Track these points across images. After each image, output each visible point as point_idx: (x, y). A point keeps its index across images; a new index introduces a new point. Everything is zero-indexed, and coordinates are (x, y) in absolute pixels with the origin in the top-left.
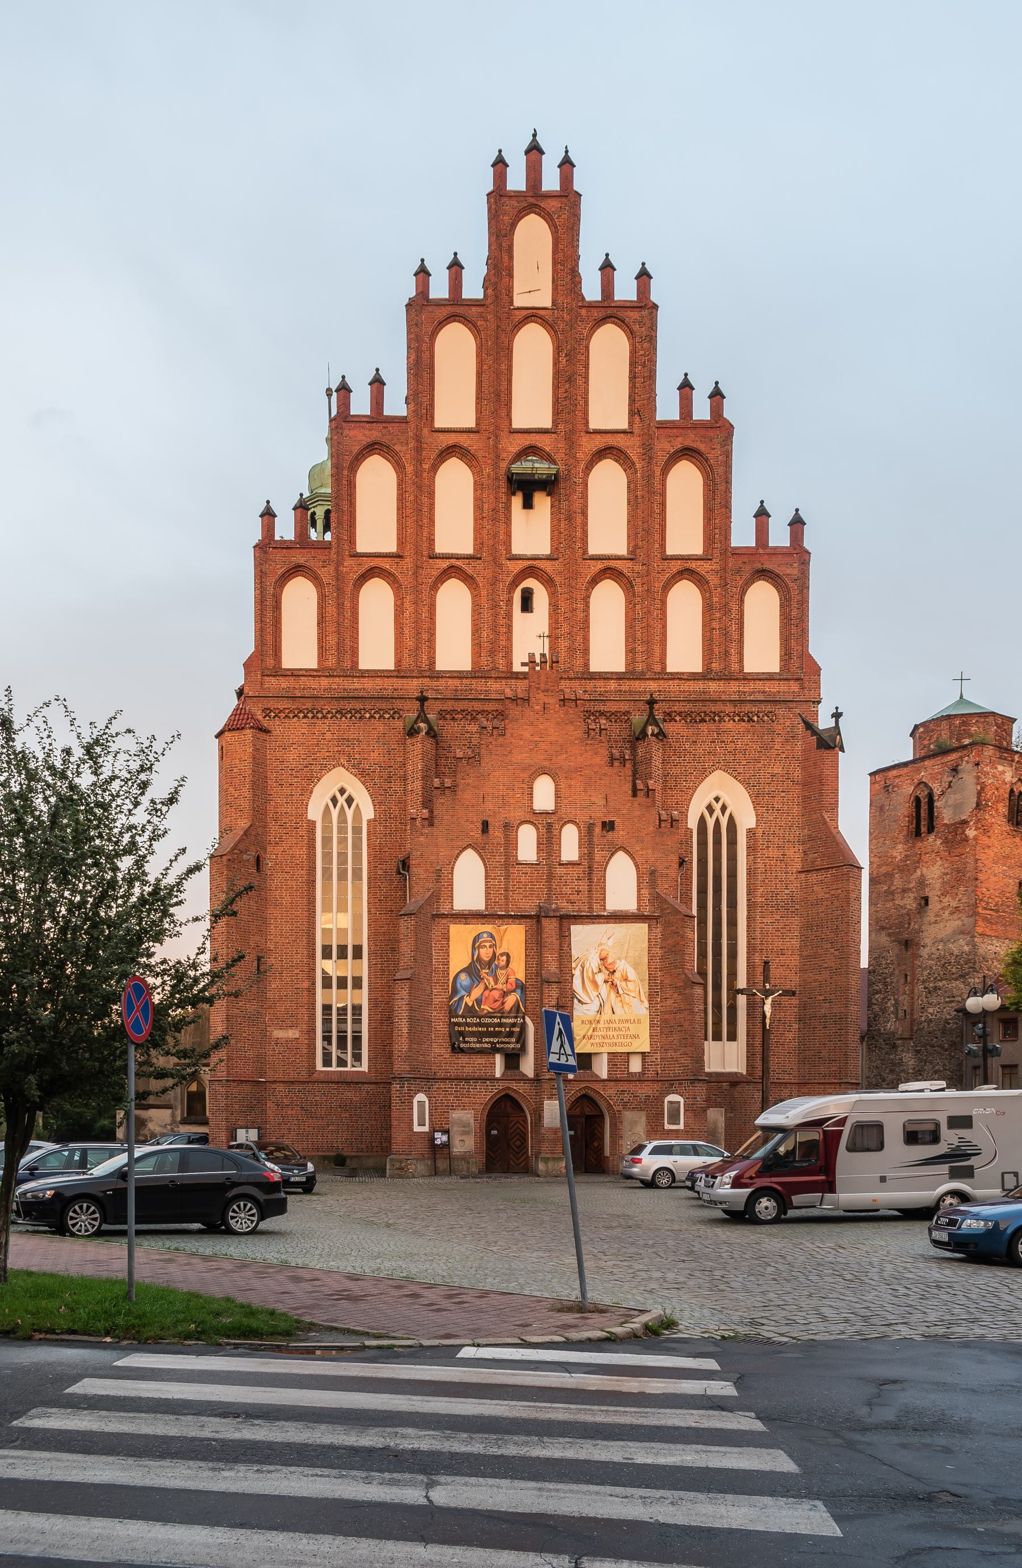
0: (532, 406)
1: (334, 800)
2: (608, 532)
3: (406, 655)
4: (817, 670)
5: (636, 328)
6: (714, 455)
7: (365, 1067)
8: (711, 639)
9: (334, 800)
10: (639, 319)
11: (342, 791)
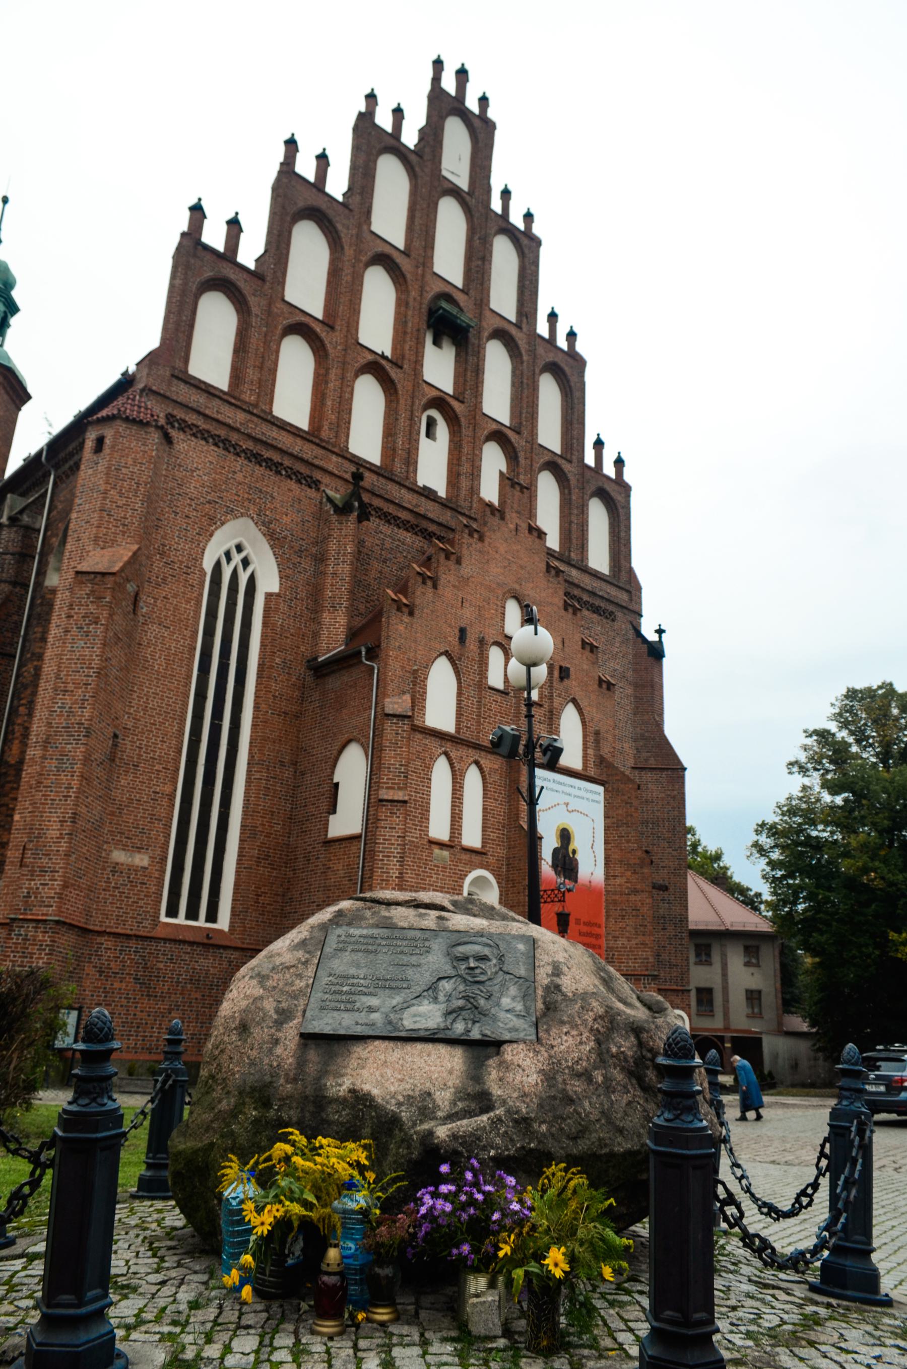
1: (228, 555)
3: (326, 427)
4: (639, 589)
5: (526, 251)
6: (573, 379)
7: (223, 922)
8: (570, 532)
9: (228, 555)
10: (527, 245)
11: (239, 548)
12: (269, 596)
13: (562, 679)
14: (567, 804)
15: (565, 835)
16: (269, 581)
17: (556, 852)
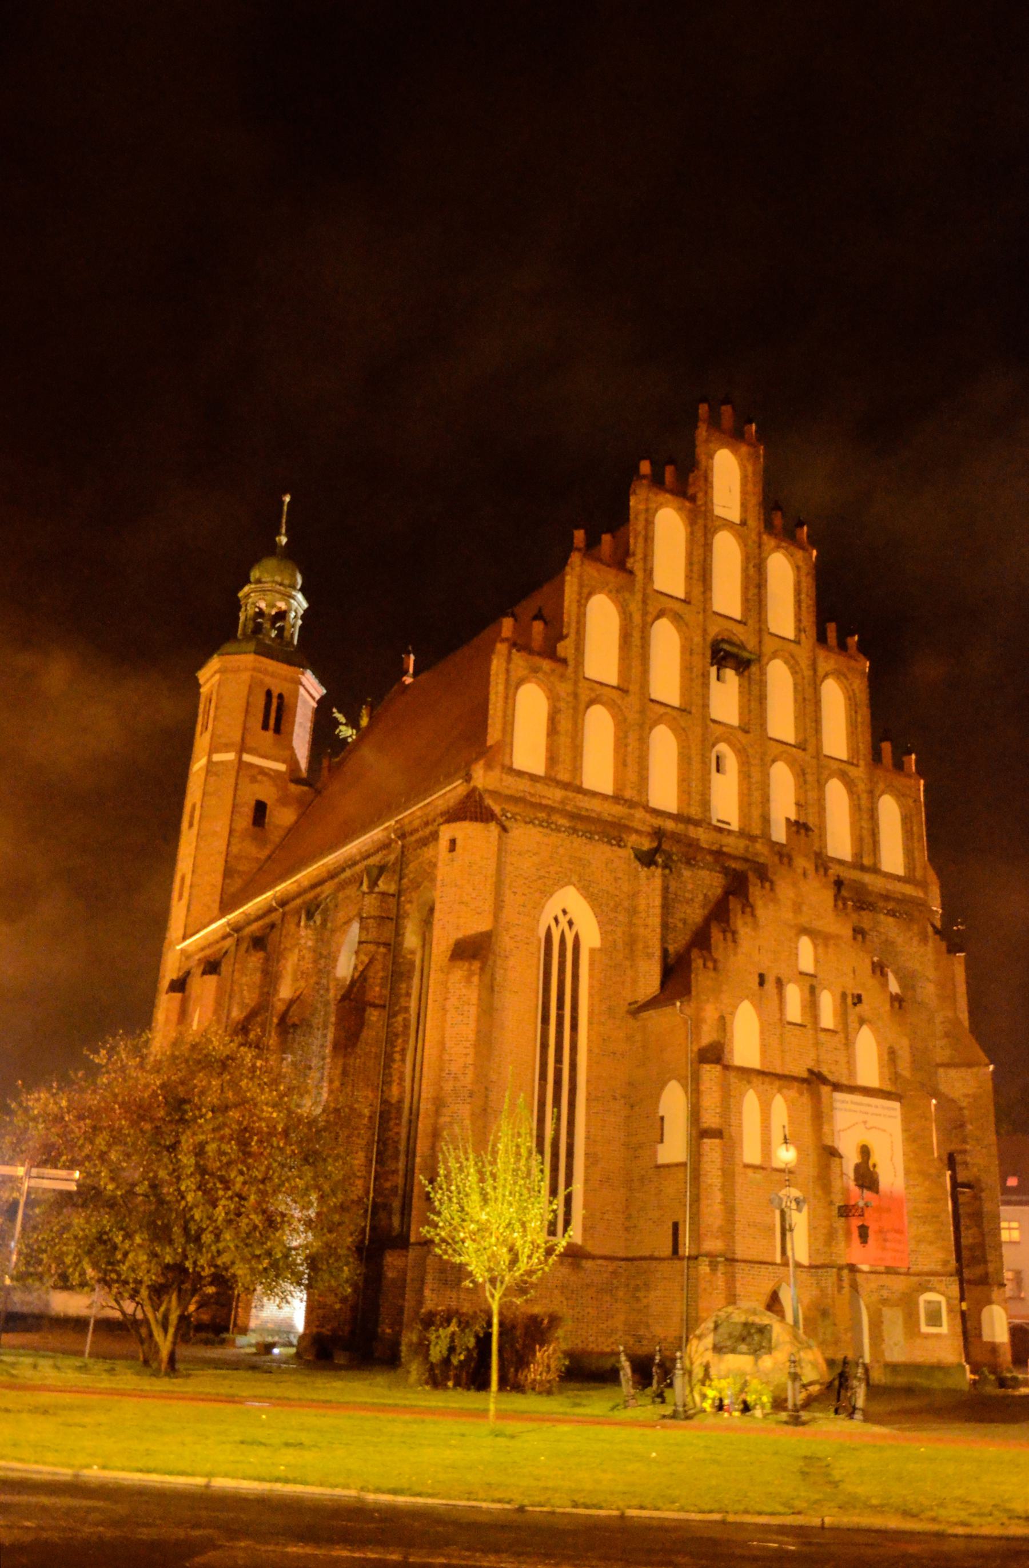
0: (727, 598)
1: (556, 919)
2: (782, 722)
11: (564, 912)
12: (592, 951)
13: (855, 1004)
14: (865, 1122)
15: (865, 1152)
16: (591, 936)
17: (857, 1167)
